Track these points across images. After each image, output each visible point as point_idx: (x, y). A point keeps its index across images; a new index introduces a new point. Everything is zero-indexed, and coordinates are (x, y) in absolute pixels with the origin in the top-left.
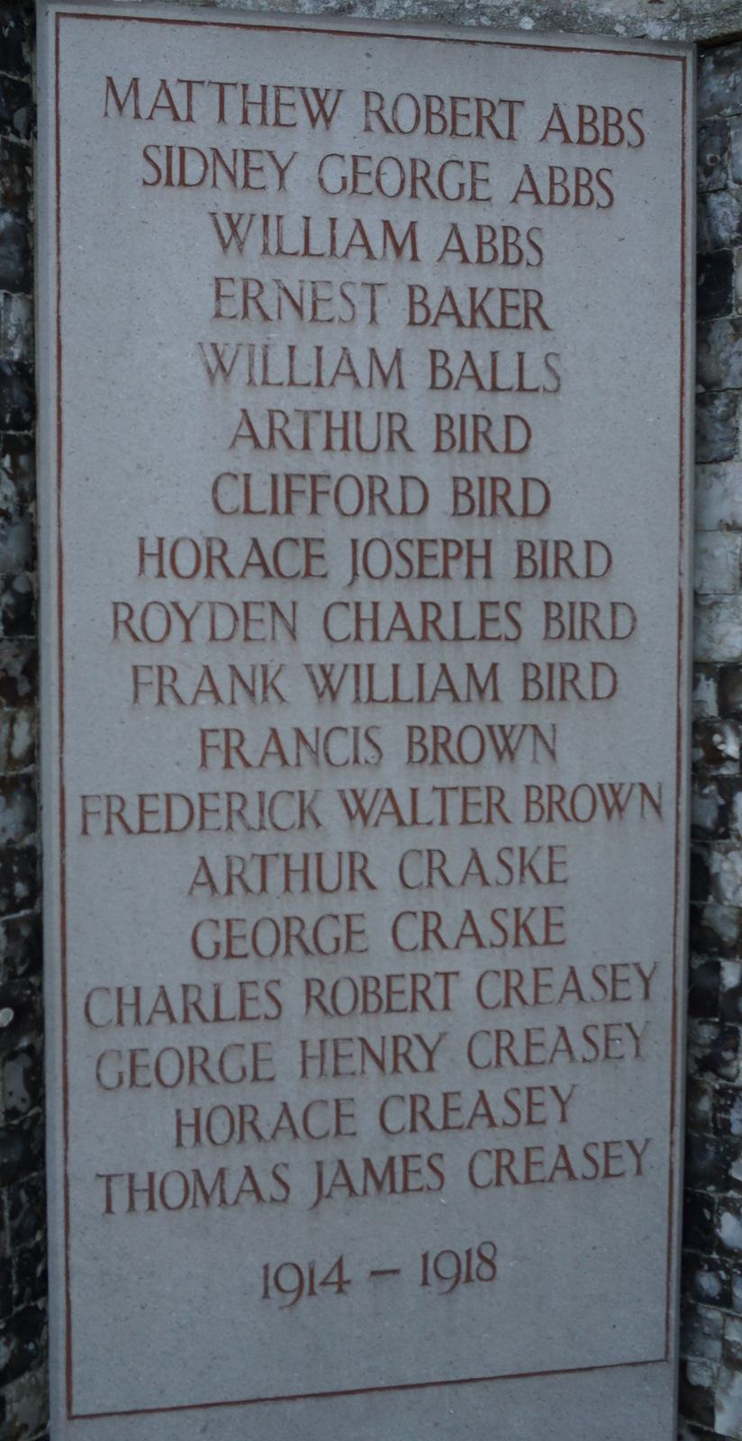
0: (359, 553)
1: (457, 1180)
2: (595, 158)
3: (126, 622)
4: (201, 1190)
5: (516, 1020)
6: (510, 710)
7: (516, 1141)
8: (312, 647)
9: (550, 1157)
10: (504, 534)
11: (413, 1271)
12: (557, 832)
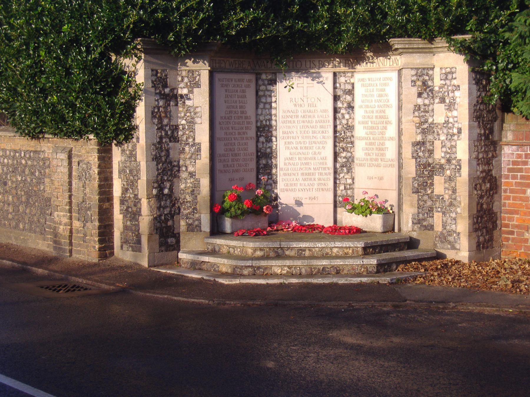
0: (234, 117)
1: (241, 171)
2: (249, 83)
3: (220, 123)
4: (225, 171)
5: (245, 157)
6: (244, 130)
7: (245, 168)
8: (231, 125)
9: (247, 169)
10: (244, 115)
11: (238, 179)
12: (248, 141)
